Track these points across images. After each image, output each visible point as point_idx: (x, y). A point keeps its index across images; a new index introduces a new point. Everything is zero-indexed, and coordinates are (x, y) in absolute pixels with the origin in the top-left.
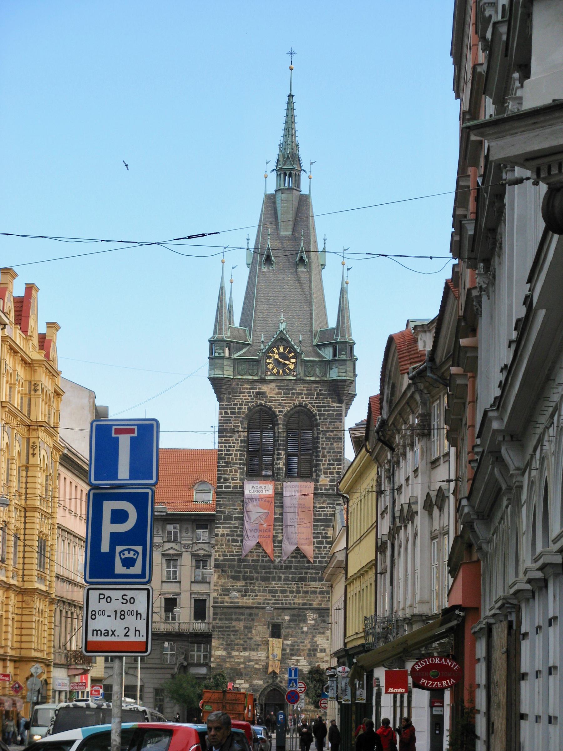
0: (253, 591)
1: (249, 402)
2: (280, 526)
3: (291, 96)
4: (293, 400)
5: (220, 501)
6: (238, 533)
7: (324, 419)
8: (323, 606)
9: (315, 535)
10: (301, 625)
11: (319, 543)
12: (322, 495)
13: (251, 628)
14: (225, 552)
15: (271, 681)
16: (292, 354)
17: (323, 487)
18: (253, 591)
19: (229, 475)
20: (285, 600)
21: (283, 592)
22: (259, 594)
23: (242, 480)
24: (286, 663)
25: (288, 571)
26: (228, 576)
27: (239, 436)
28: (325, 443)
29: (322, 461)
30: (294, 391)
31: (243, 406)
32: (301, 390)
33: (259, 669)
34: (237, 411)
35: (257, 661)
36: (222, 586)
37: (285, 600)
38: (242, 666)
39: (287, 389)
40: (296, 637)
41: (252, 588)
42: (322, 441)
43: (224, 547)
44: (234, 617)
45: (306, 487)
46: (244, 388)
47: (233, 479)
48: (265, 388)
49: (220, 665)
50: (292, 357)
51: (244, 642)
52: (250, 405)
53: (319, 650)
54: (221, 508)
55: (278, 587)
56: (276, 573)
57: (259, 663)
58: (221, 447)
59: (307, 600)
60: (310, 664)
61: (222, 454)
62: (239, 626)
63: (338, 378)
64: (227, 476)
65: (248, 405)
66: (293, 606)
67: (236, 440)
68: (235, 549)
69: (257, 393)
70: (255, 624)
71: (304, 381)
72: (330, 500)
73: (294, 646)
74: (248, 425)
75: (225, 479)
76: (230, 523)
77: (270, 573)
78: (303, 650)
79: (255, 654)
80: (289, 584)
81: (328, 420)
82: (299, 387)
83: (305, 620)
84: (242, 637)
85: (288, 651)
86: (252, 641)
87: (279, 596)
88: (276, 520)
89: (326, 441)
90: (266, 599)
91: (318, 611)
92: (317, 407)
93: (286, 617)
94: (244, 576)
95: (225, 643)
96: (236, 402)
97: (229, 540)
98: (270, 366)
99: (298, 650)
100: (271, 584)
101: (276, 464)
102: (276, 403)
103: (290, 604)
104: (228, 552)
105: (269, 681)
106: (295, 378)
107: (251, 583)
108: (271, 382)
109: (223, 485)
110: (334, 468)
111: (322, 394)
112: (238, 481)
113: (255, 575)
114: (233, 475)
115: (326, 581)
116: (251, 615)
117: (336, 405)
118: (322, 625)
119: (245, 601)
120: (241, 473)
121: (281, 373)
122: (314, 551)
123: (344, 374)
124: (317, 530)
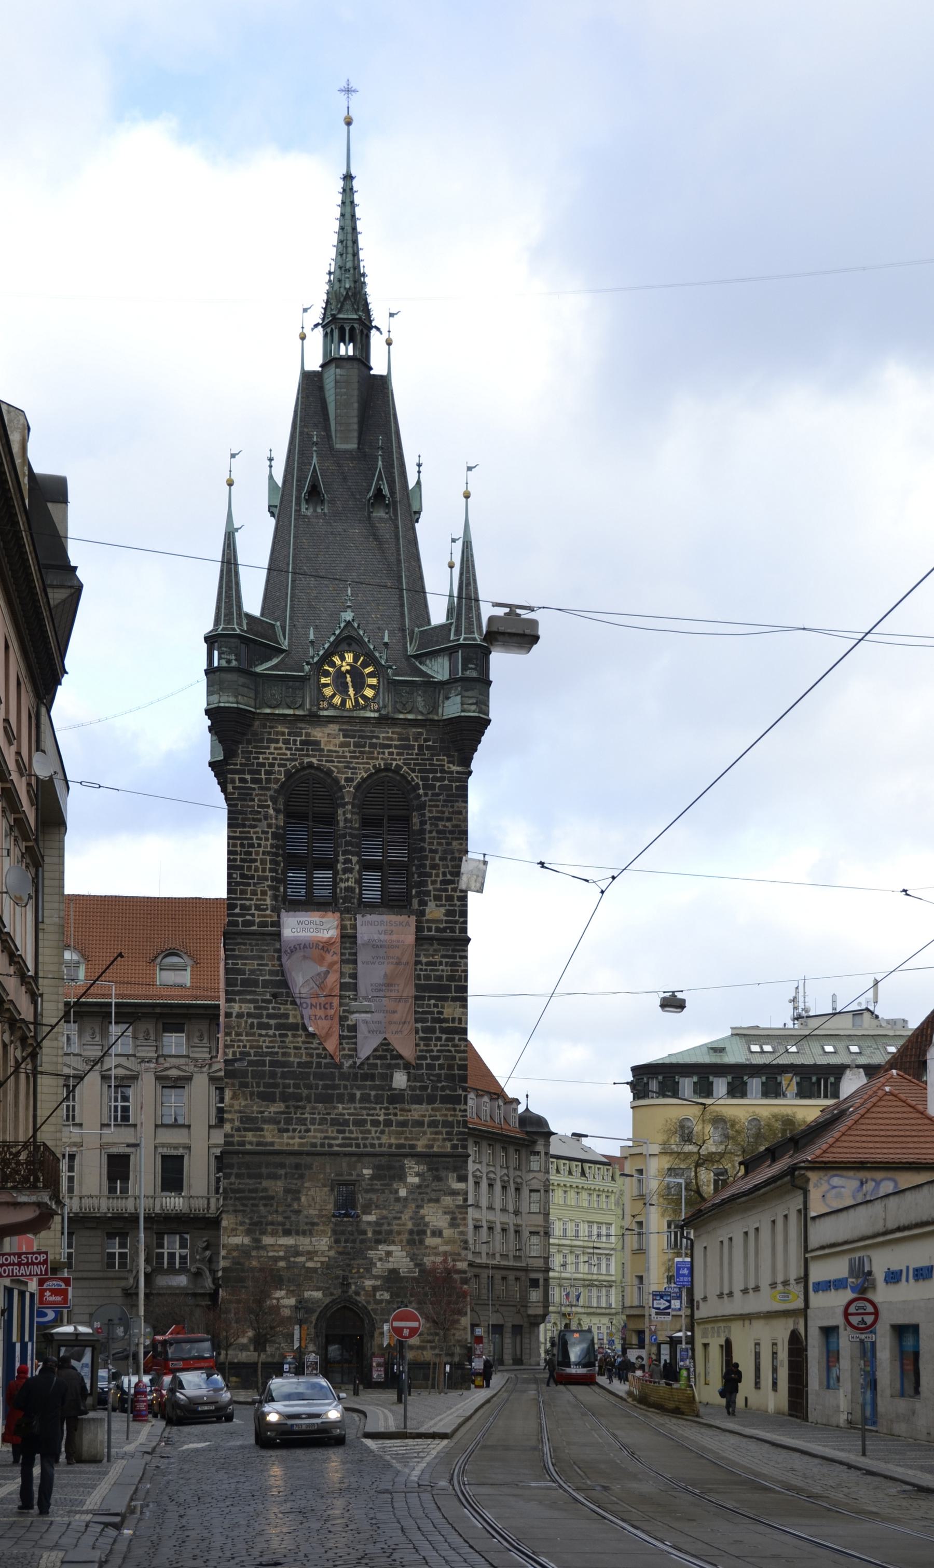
0: (302, 1121)
1: (287, 760)
3: (348, 177)
4: (372, 758)
5: (234, 950)
6: (271, 1011)
7: (433, 795)
8: (435, 1149)
10: (395, 1186)
11: (425, 1030)
12: (431, 939)
13: (299, 1192)
14: (245, 1047)
15: (338, 1292)
16: (369, 669)
17: (434, 926)
18: (302, 1121)
19: (251, 899)
20: (363, 1139)
21: (360, 1123)
23: (276, 910)
24: (367, 1258)
26: (252, 1094)
27: (269, 826)
29: (430, 875)
30: (374, 741)
31: (276, 768)
33: (315, 1270)
34: (263, 776)
35: (311, 1255)
36: (240, 1112)
37: (363, 1139)
38: (282, 1264)
39: (360, 737)
40: (385, 1208)
41: (298, 1115)
42: (430, 838)
43: (244, 1038)
44: (264, 1170)
45: (401, 924)
46: (277, 733)
47: (258, 908)
48: (318, 734)
49: (238, 1263)
50: (371, 675)
51: (285, 1218)
52: (289, 767)
53: (428, 1232)
54: (237, 964)
55: (349, 1114)
56: (345, 1087)
58: (235, 845)
59: (406, 1139)
60: (412, 1260)
61: (235, 860)
62: (277, 1187)
63: (463, 714)
64: (248, 903)
65: (285, 765)
66: (377, 1149)
67: (263, 832)
68: (264, 1041)
69: (302, 743)
70: (306, 1185)
71: (394, 722)
72: (448, 950)
73: (383, 1224)
74: (286, 805)
75: (243, 907)
76: (254, 993)
77: (335, 1087)
78: (399, 1233)
79: (306, 1241)
80: (370, 1109)
81: (441, 797)
82: (385, 734)
83: (402, 1177)
84: (280, 1209)
85: (370, 1235)
86: (300, 1217)
87: (351, 1132)
88: (343, 986)
89: (439, 838)
90: (325, 1138)
91: (428, 1159)
92: (420, 771)
93: (365, 1171)
95: (247, 1221)
96: (261, 760)
97: (252, 1023)
98: (328, 692)
99: (390, 1232)
100: (335, 1108)
101: (341, 880)
103: (373, 1146)
104: (251, 1047)
105: (335, 1292)
106: (376, 715)
107: (297, 1107)
108: (333, 722)
109: (240, 919)
111: (428, 748)
112: (268, 912)
113: (305, 1092)
114: (257, 900)
115: (441, 1103)
116: (297, 1166)
117: (455, 768)
118: (434, 1185)
119: (286, 1140)
120: (275, 898)
121: (349, 704)
122: (417, 1045)
123: (473, 707)
124: (422, 1006)
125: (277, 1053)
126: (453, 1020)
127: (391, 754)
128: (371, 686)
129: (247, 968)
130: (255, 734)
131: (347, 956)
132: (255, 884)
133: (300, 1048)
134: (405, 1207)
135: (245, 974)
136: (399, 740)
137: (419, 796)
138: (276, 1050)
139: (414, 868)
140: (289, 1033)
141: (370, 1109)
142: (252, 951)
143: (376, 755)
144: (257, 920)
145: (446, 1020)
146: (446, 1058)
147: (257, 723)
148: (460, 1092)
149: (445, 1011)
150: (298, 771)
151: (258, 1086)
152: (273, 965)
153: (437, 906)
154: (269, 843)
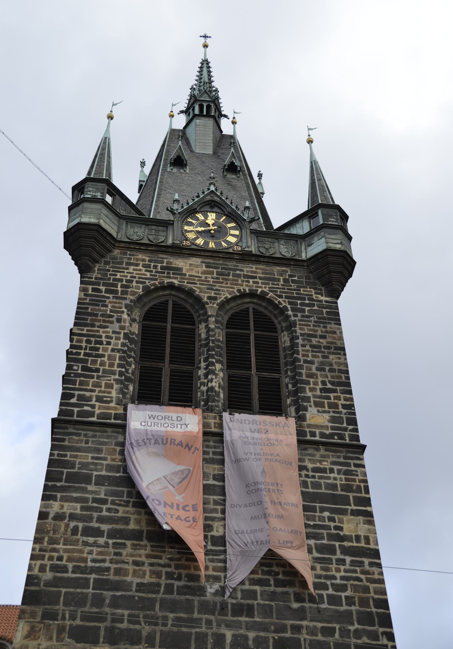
2: (216, 503)
5: (63, 440)
6: (105, 513)
7: (302, 316)
9: (309, 530)
11: (320, 549)
14: (60, 558)
25: (243, 619)
26: (61, 629)
27: (122, 328)
28: (310, 354)
29: (308, 383)
30: (238, 272)
31: (134, 284)
32: (252, 272)
34: (119, 289)
39: (222, 268)
43: (61, 546)
46: (137, 259)
47: (99, 399)
52: (147, 284)
54: (66, 456)
56: (209, 622)
58: (81, 341)
64: (88, 394)
65: (145, 283)
67: (114, 332)
68: (90, 553)
72: (339, 457)
76: (84, 490)
82: (248, 268)
89: (312, 351)
92: (286, 297)
94: (110, 631)
96: (118, 277)
102: (200, 284)
104: (70, 560)
109: (76, 410)
110: (338, 398)
111: (293, 281)
112: (113, 405)
113: (146, 629)
114: (100, 392)
117: (323, 298)
125: (108, 569)
126: (358, 538)
127: (254, 282)
128: (233, 235)
129: (78, 461)
130: (115, 258)
131: (211, 455)
132: (98, 377)
133: (143, 564)
135: (74, 468)
136: (263, 273)
137: (288, 317)
138: (107, 565)
139: (287, 380)
140: (128, 543)
142: (87, 442)
143: (240, 282)
144: (97, 411)
146: (355, 588)
147: (116, 252)
148: (384, 641)
149: (345, 526)
150: (157, 289)
151: (73, 618)
152: (113, 460)
153: (318, 411)
154: (120, 342)
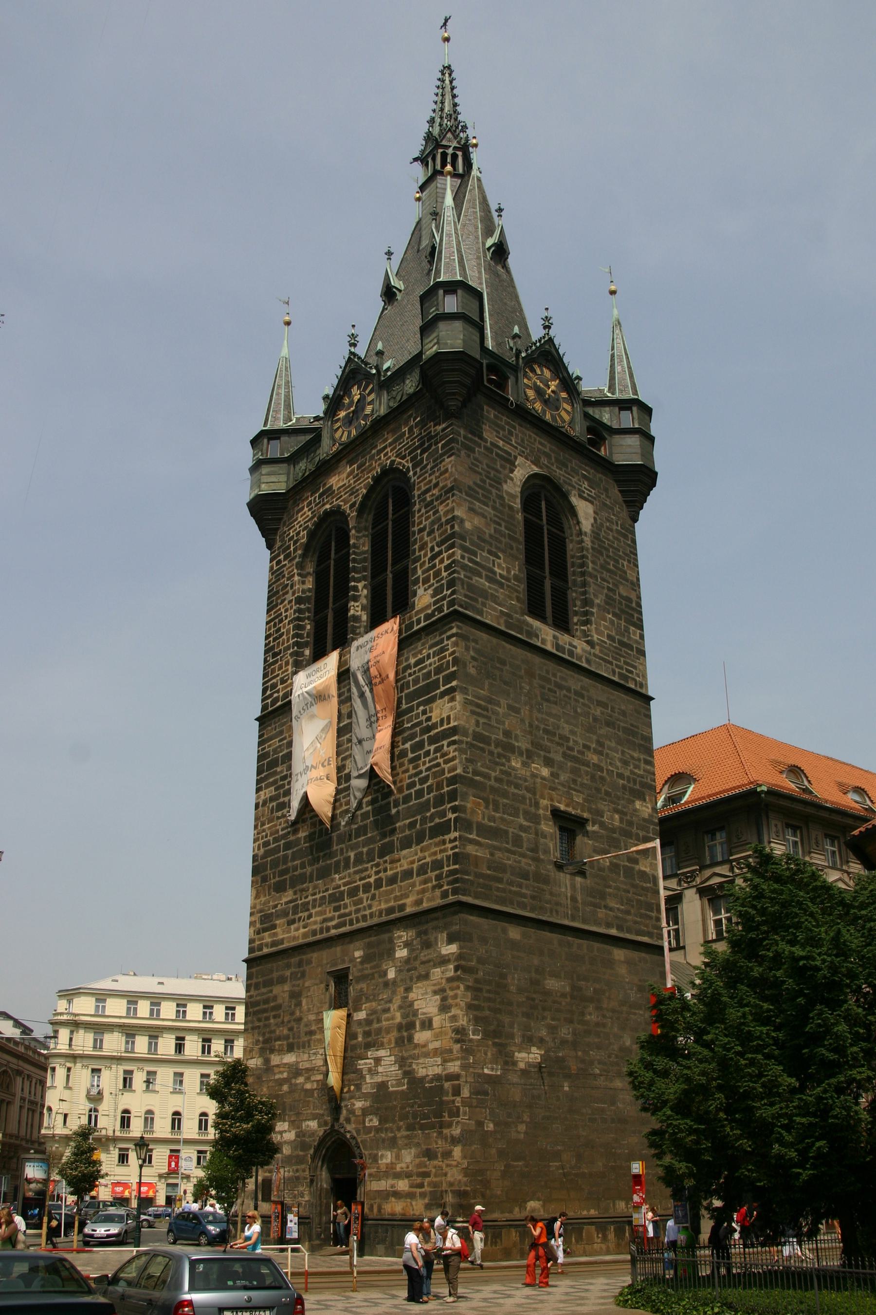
22: (313, 911)
33: (312, 1090)
38: (285, 1088)
41: (303, 900)
57: (313, 1078)
60: (401, 1067)
70: (307, 984)
78: (388, 1031)
80: (362, 871)
84: (286, 1020)
90: (325, 920)
118: (424, 955)
134: (394, 993)
141: (362, 871)
145: (434, 726)
